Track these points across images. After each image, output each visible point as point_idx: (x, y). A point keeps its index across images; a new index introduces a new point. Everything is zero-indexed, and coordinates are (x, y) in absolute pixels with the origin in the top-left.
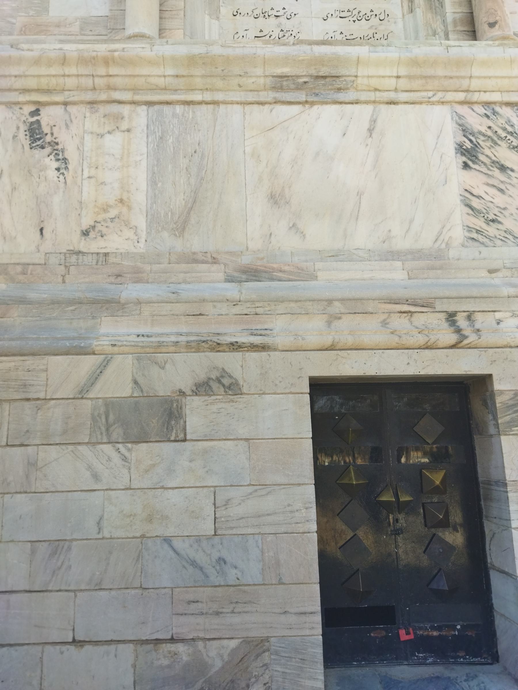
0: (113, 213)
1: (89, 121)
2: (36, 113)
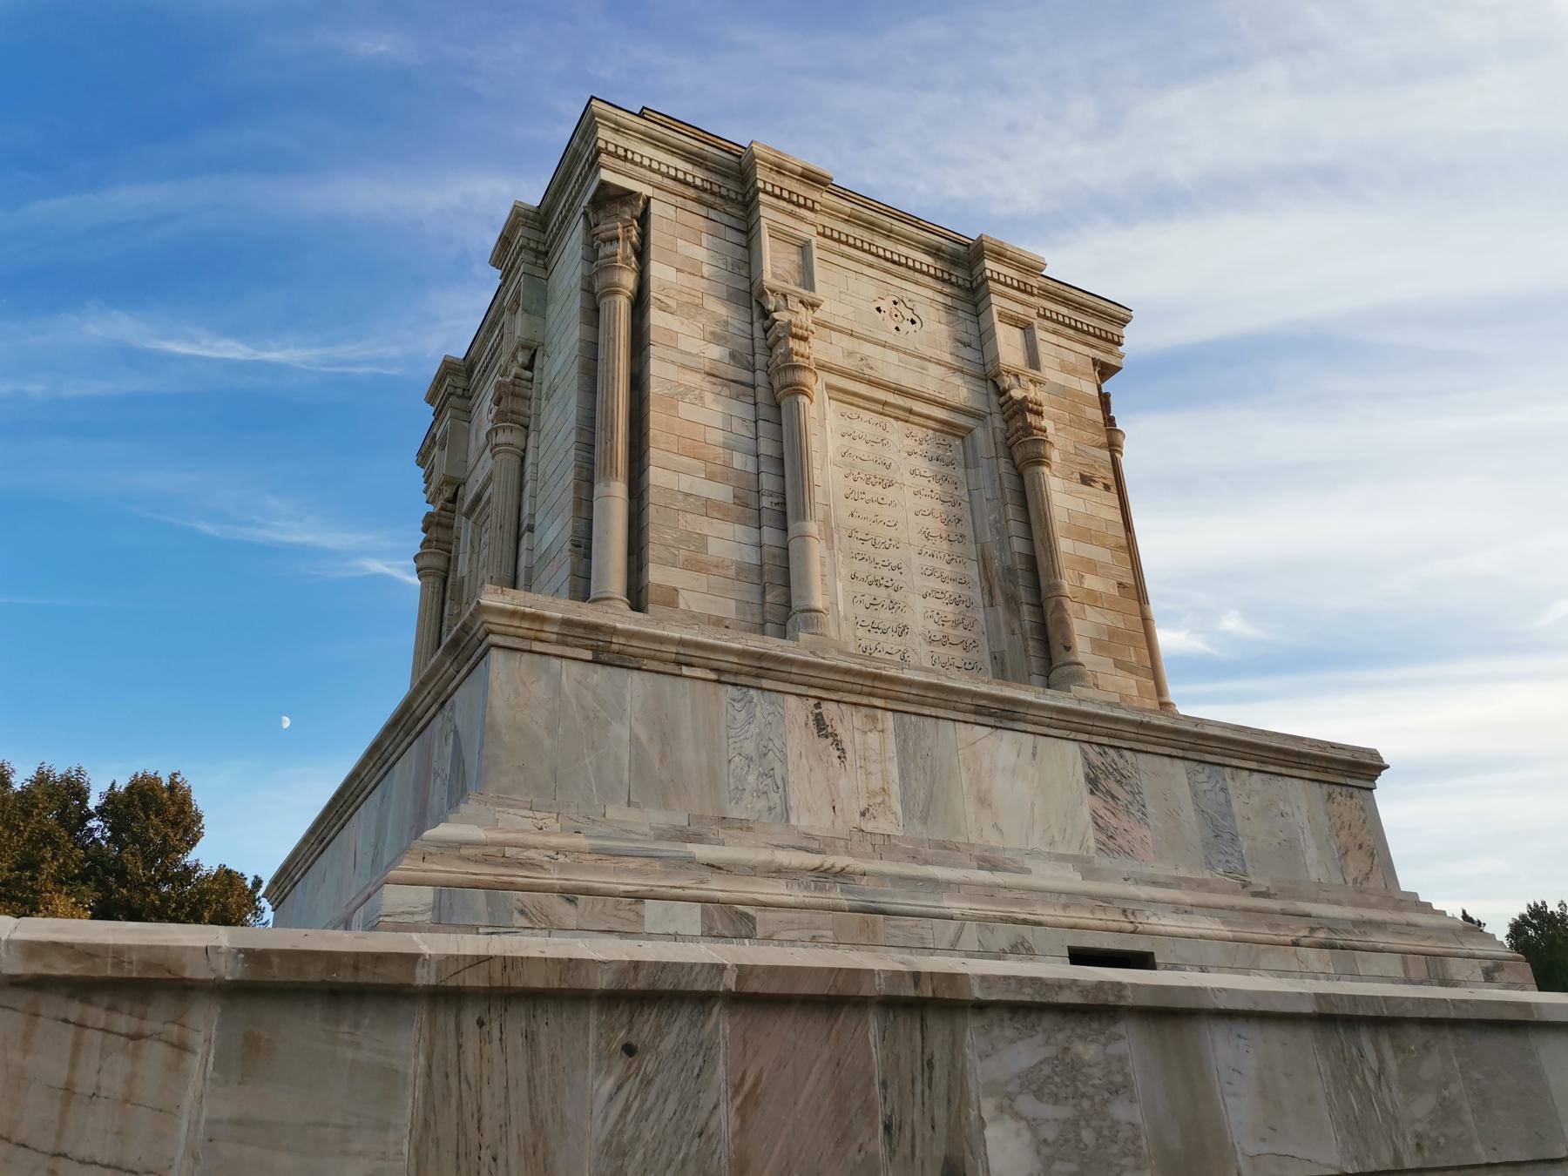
0: (879, 800)
1: (857, 718)
2: (818, 706)
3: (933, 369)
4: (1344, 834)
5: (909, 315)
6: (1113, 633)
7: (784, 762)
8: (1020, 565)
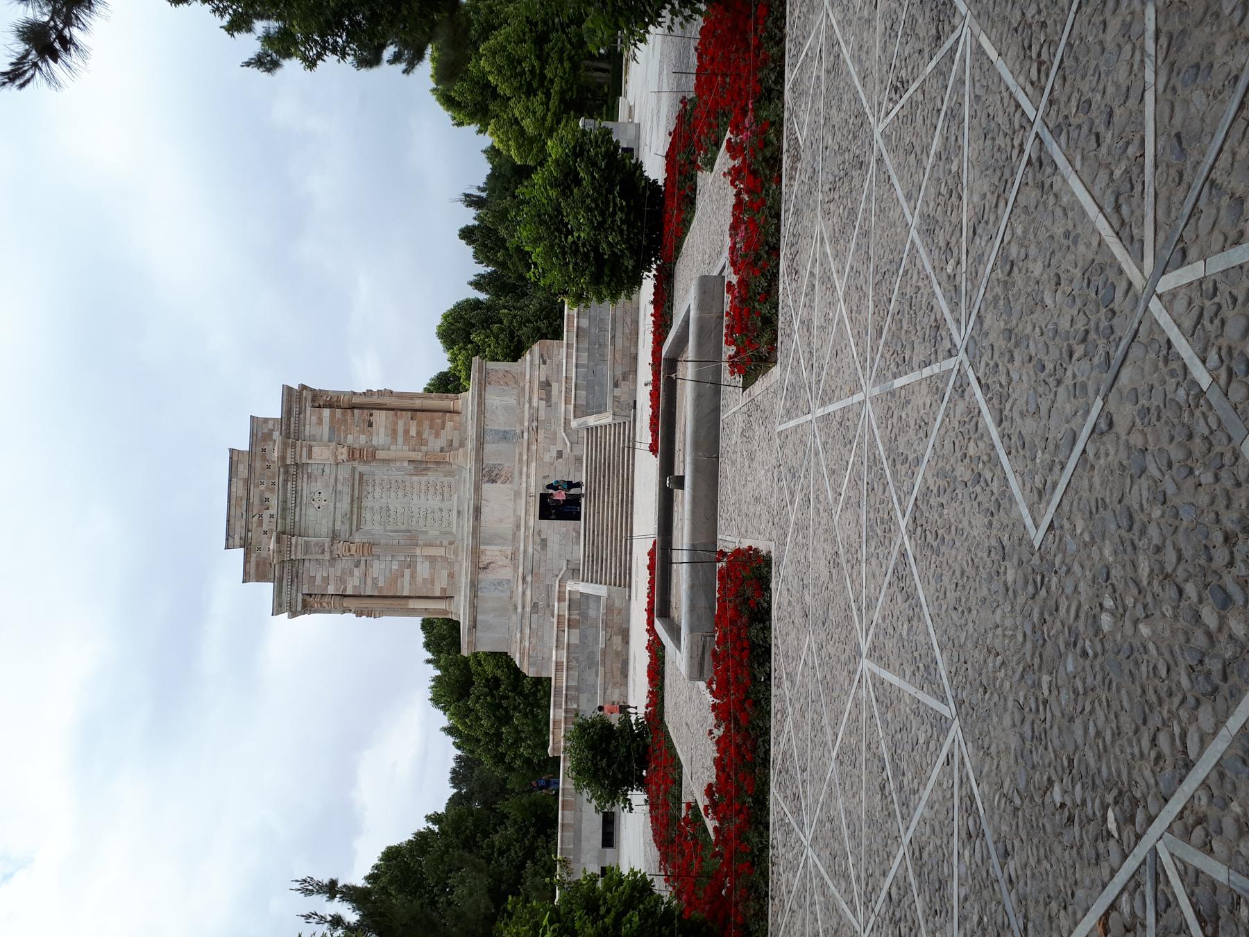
1: (483, 558)
3: (339, 487)
6: (431, 427)
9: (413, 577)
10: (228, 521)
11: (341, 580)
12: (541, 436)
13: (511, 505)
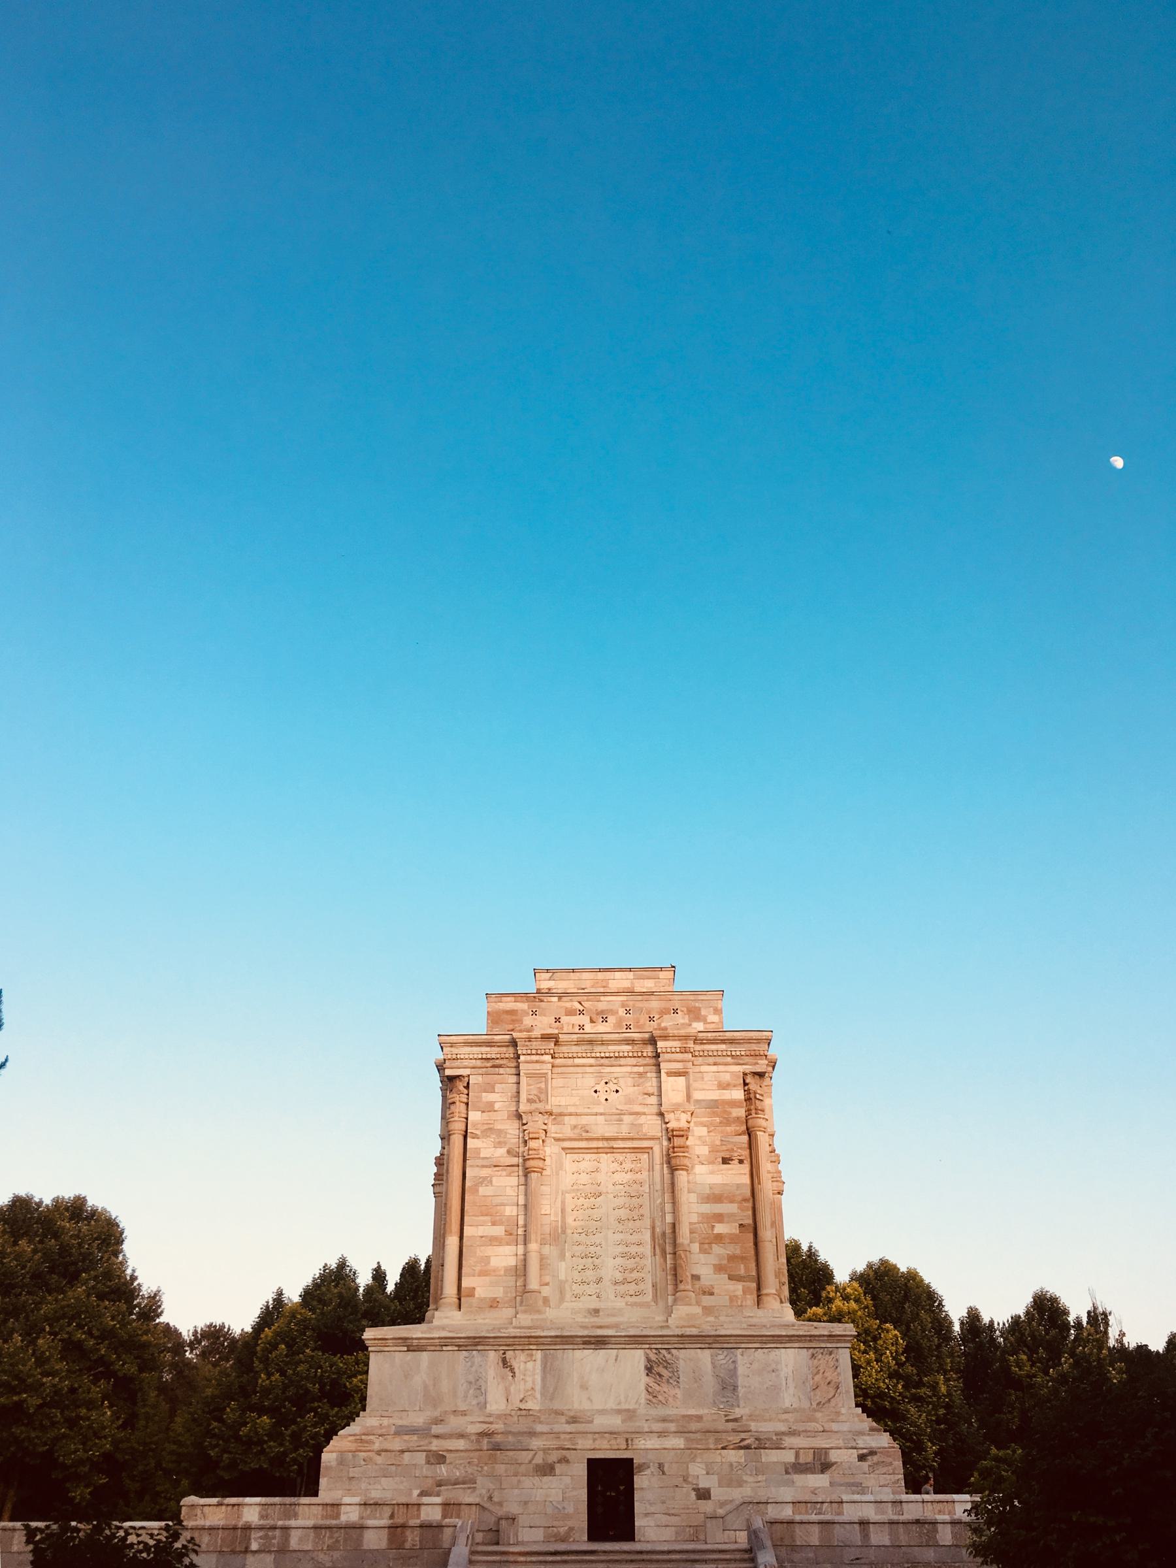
1: (522, 1356)
3: (627, 1119)
4: (817, 1378)
5: (615, 1087)
6: (732, 1258)
7: (486, 1382)
8: (668, 1231)
9: (494, 1241)
10: (573, 971)
11: (489, 1131)
12: (734, 1456)
13: (611, 1405)
